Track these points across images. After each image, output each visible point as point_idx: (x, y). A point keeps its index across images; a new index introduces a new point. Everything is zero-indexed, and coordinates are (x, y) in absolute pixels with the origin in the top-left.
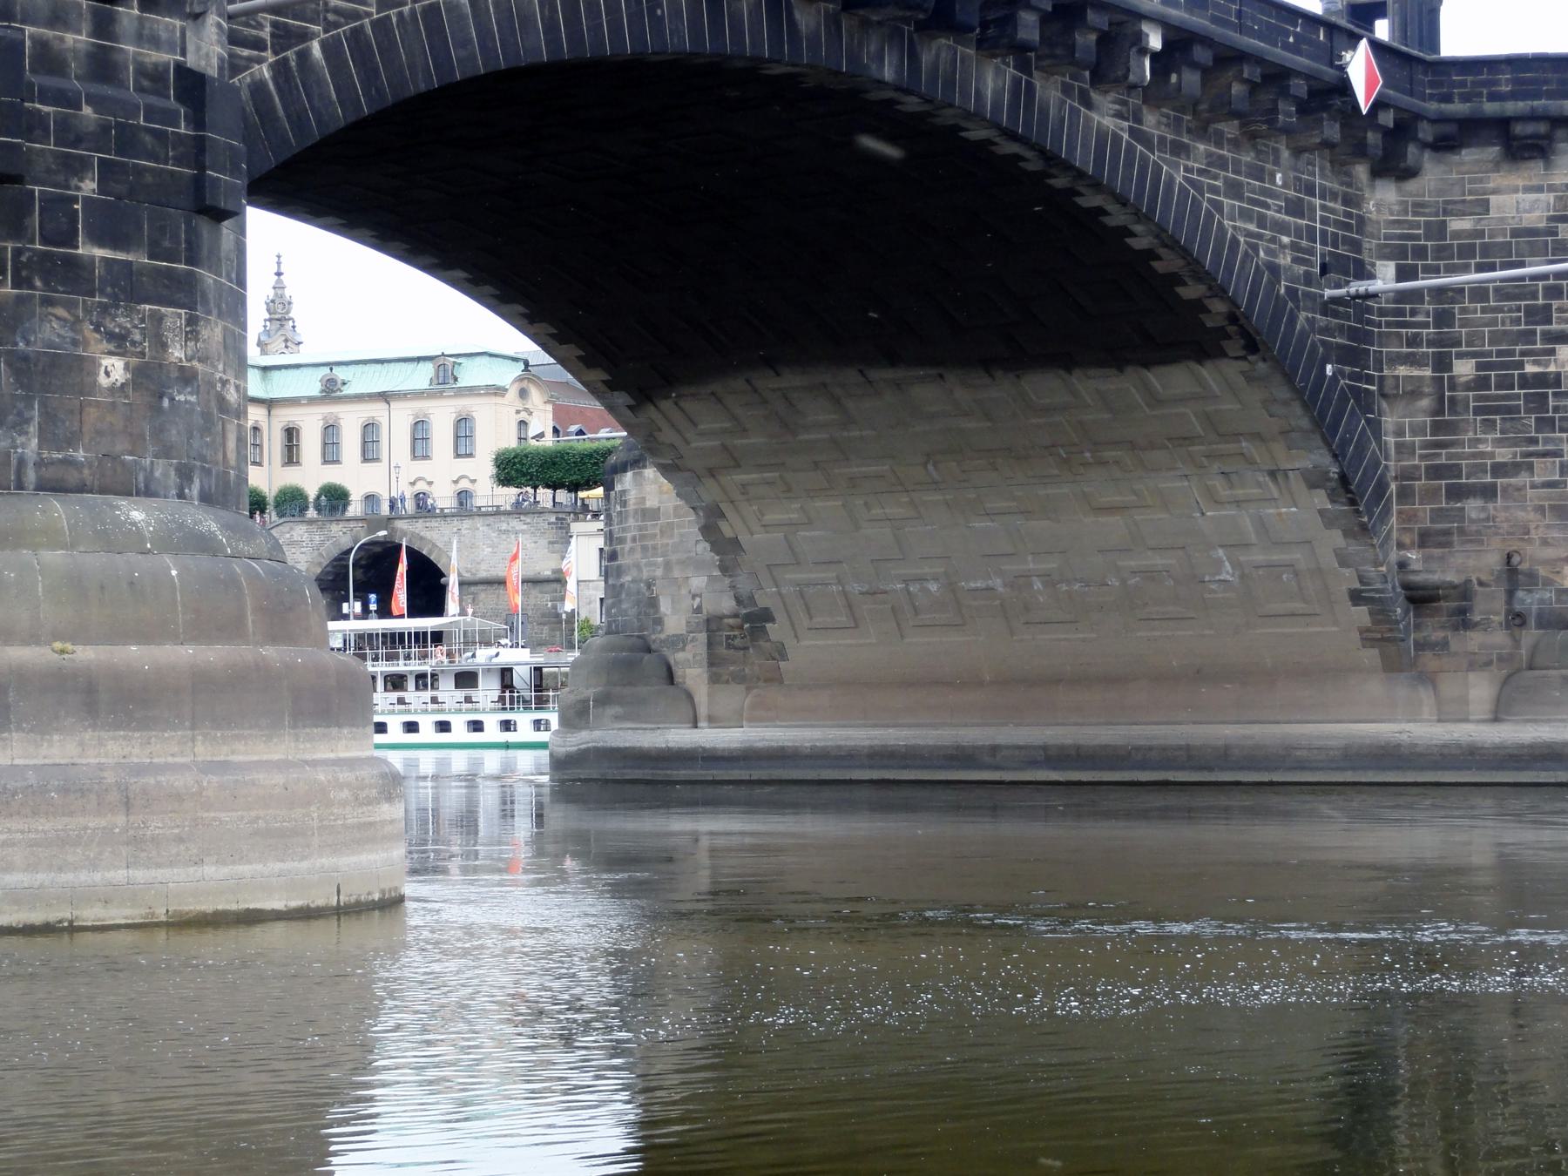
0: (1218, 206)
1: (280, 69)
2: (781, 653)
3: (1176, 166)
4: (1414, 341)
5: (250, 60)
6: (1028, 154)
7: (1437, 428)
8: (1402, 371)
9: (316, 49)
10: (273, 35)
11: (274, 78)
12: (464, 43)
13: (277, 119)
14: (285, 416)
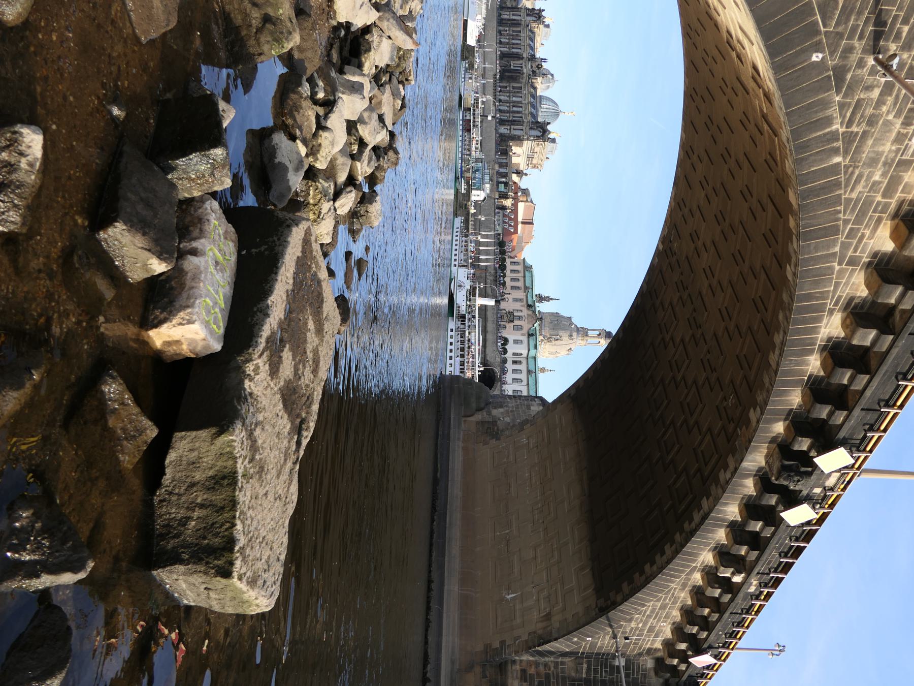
0: (658, 601)
1: (834, 136)
2: (485, 443)
3: (678, 585)
4: (596, 671)
5: (845, 116)
6: (693, 525)
7: (563, 678)
8: (585, 666)
9: (838, 159)
10: (852, 132)
11: (831, 132)
12: (817, 249)
13: (811, 133)
14: (524, 361)
